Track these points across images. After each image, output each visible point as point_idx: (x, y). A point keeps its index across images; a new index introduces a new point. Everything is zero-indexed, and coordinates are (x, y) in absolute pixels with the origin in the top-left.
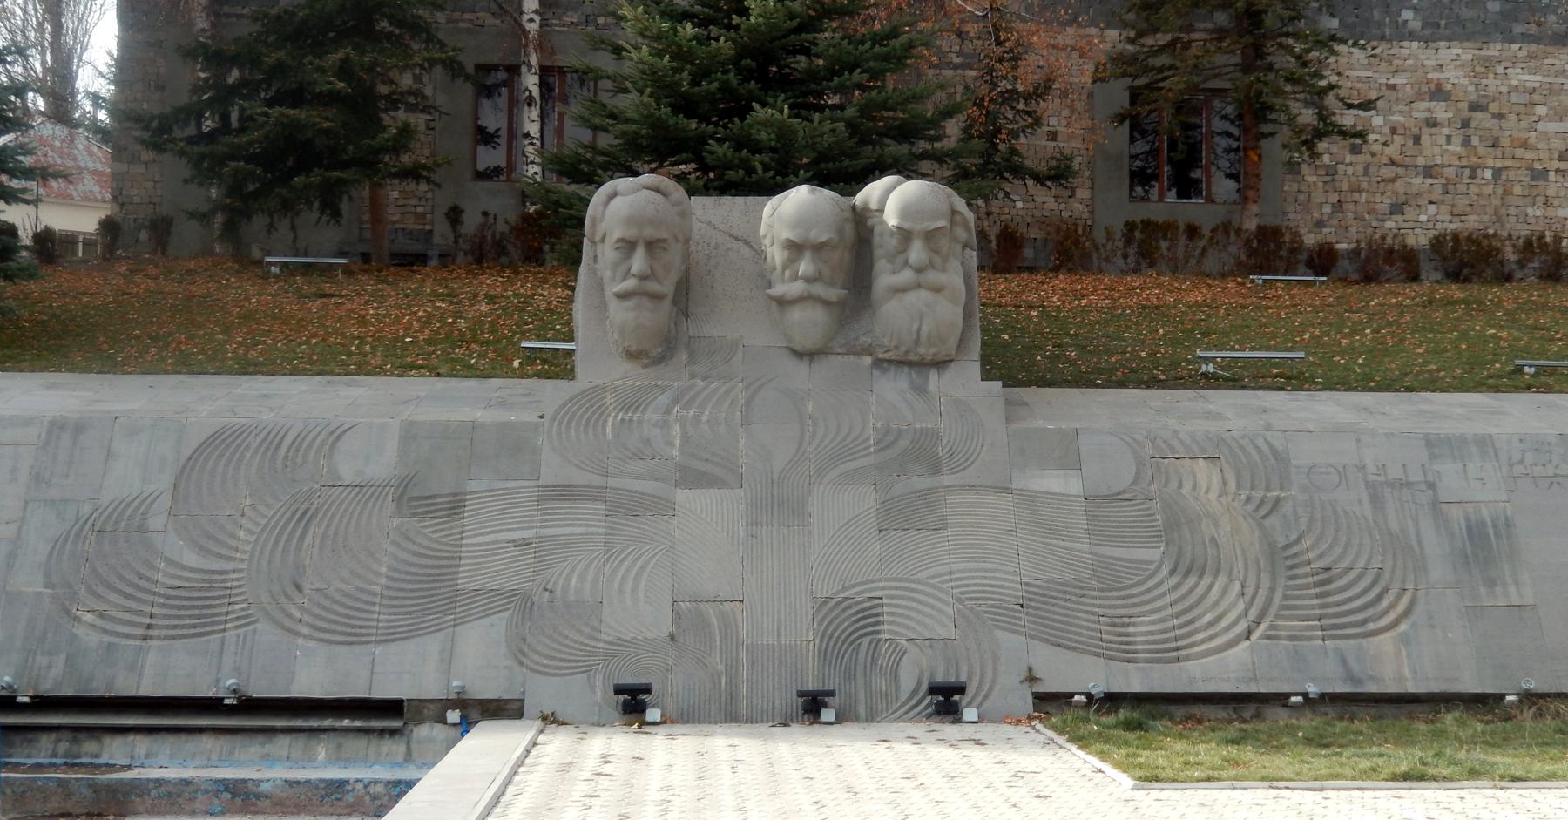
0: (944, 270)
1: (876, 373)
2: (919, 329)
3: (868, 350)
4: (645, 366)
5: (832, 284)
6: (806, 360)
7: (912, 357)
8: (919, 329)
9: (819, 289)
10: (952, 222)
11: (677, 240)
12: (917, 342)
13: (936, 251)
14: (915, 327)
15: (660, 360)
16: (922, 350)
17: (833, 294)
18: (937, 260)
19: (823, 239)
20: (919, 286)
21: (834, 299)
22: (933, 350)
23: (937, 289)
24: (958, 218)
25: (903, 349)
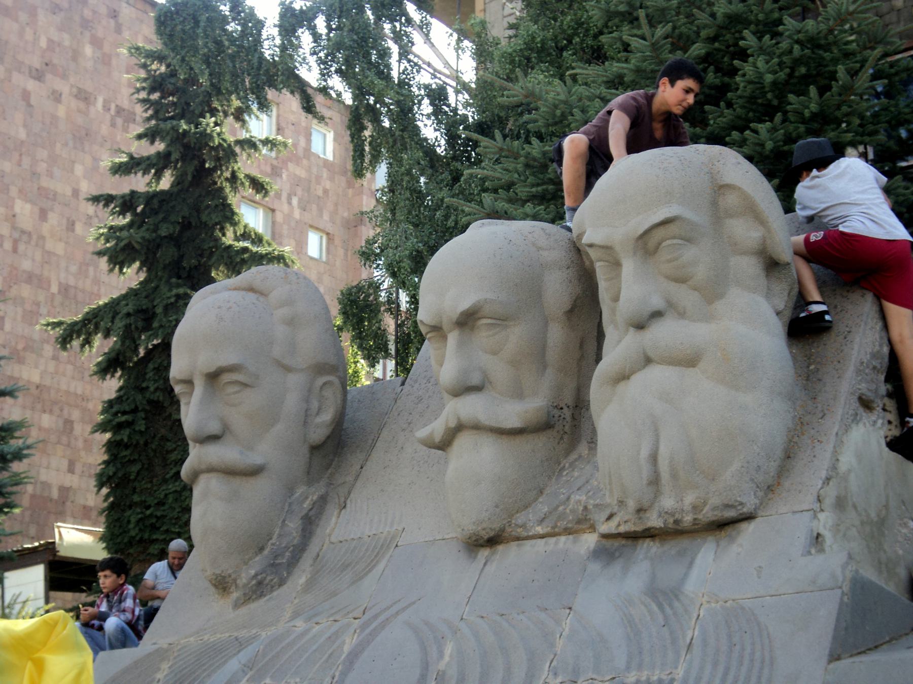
0: (708, 318)
1: (595, 567)
2: (654, 458)
3: (582, 523)
4: (237, 605)
5: (518, 393)
6: (484, 553)
7: (654, 521)
8: (654, 458)
9: (471, 407)
10: (718, 215)
11: (288, 369)
12: (655, 481)
13: (681, 280)
14: (645, 452)
15: (259, 589)
16: (668, 502)
17: (512, 413)
18: (686, 297)
19: (465, 304)
20: (648, 361)
21: (514, 422)
22: (689, 499)
23: (690, 361)
24: (731, 200)
25: (632, 504)
